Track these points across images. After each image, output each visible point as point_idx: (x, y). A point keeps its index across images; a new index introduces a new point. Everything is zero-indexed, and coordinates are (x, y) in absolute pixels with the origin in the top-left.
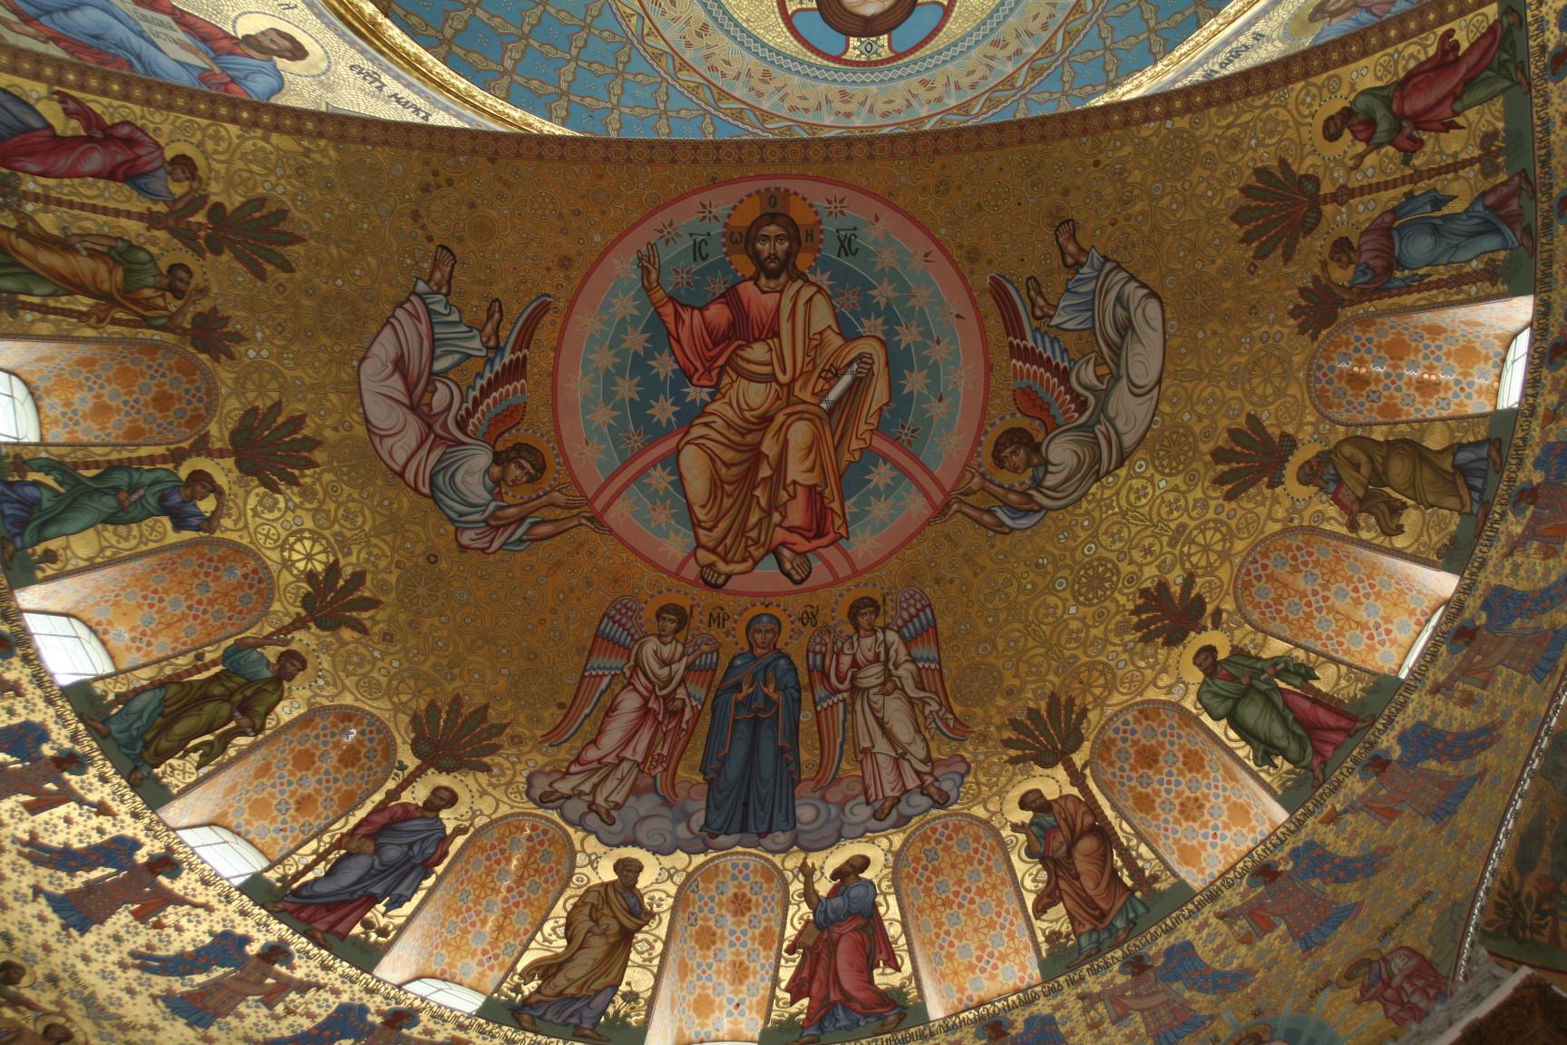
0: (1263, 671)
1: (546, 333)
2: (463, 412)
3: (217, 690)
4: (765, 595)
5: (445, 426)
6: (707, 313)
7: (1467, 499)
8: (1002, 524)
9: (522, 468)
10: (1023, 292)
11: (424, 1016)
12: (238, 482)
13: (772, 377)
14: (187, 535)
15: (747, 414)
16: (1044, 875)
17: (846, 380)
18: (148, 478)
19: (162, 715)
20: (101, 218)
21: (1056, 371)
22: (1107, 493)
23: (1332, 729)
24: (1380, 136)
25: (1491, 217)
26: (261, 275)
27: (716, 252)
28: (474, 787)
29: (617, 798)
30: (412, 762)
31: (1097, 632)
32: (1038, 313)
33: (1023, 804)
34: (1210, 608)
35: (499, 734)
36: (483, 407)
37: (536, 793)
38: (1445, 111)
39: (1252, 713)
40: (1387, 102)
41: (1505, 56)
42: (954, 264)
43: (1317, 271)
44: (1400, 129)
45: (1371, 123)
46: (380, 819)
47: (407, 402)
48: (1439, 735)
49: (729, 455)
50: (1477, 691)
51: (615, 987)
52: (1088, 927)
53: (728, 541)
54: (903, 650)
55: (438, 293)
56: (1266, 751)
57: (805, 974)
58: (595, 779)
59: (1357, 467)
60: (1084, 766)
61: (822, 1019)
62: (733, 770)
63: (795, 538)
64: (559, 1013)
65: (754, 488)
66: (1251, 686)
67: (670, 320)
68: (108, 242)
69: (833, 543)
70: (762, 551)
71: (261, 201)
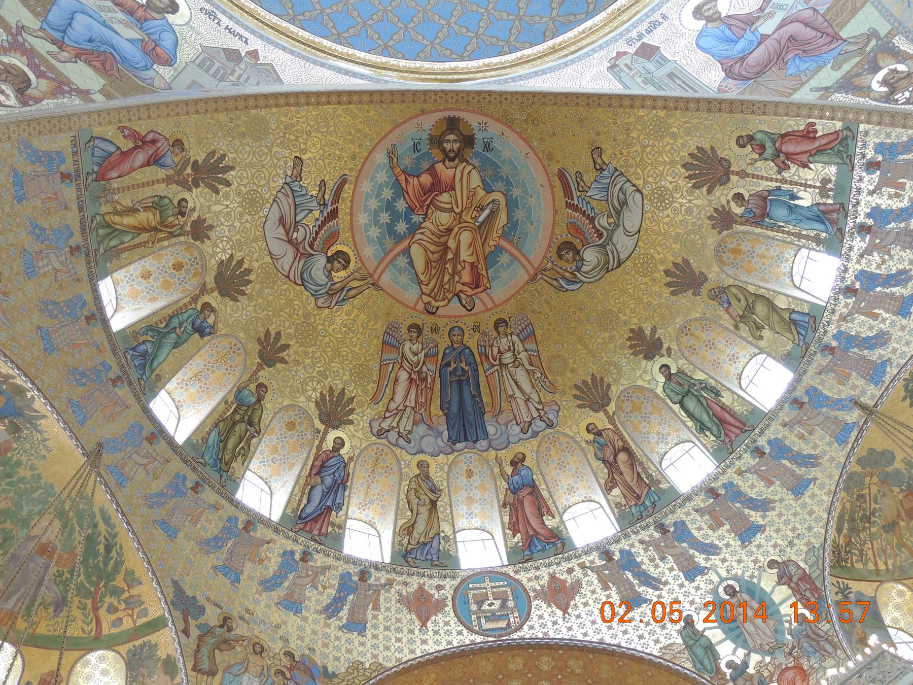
3: (238, 417)
4: (455, 317)
5: (304, 248)
7: (796, 337)
8: (563, 287)
9: (340, 262)
11: (372, 571)
13: (452, 210)
14: (206, 338)
15: (441, 228)
16: (606, 470)
17: (487, 212)
18: (186, 316)
19: (221, 441)
20: (146, 189)
23: (732, 425)
24: (766, 155)
25: (821, 215)
26: (217, 192)
27: (425, 147)
29: (409, 428)
30: (322, 427)
31: (611, 346)
32: (581, 189)
34: (665, 346)
35: (352, 403)
36: (320, 235)
37: (375, 431)
38: (804, 158)
39: (691, 404)
40: (774, 142)
41: (841, 148)
42: (541, 161)
44: (778, 156)
45: (763, 147)
46: (318, 463)
48: (789, 449)
50: (806, 434)
51: (439, 534)
52: (633, 503)
53: (436, 290)
54: (521, 346)
56: (702, 428)
57: (514, 520)
58: (397, 419)
59: (739, 301)
60: (614, 414)
61: (529, 545)
62: (455, 408)
63: (466, 288)
66: (689, 391)
67: (403, 183)
68: (150, 200)
69: (484, 291)
70: (451, 295)
71: (213, 153)
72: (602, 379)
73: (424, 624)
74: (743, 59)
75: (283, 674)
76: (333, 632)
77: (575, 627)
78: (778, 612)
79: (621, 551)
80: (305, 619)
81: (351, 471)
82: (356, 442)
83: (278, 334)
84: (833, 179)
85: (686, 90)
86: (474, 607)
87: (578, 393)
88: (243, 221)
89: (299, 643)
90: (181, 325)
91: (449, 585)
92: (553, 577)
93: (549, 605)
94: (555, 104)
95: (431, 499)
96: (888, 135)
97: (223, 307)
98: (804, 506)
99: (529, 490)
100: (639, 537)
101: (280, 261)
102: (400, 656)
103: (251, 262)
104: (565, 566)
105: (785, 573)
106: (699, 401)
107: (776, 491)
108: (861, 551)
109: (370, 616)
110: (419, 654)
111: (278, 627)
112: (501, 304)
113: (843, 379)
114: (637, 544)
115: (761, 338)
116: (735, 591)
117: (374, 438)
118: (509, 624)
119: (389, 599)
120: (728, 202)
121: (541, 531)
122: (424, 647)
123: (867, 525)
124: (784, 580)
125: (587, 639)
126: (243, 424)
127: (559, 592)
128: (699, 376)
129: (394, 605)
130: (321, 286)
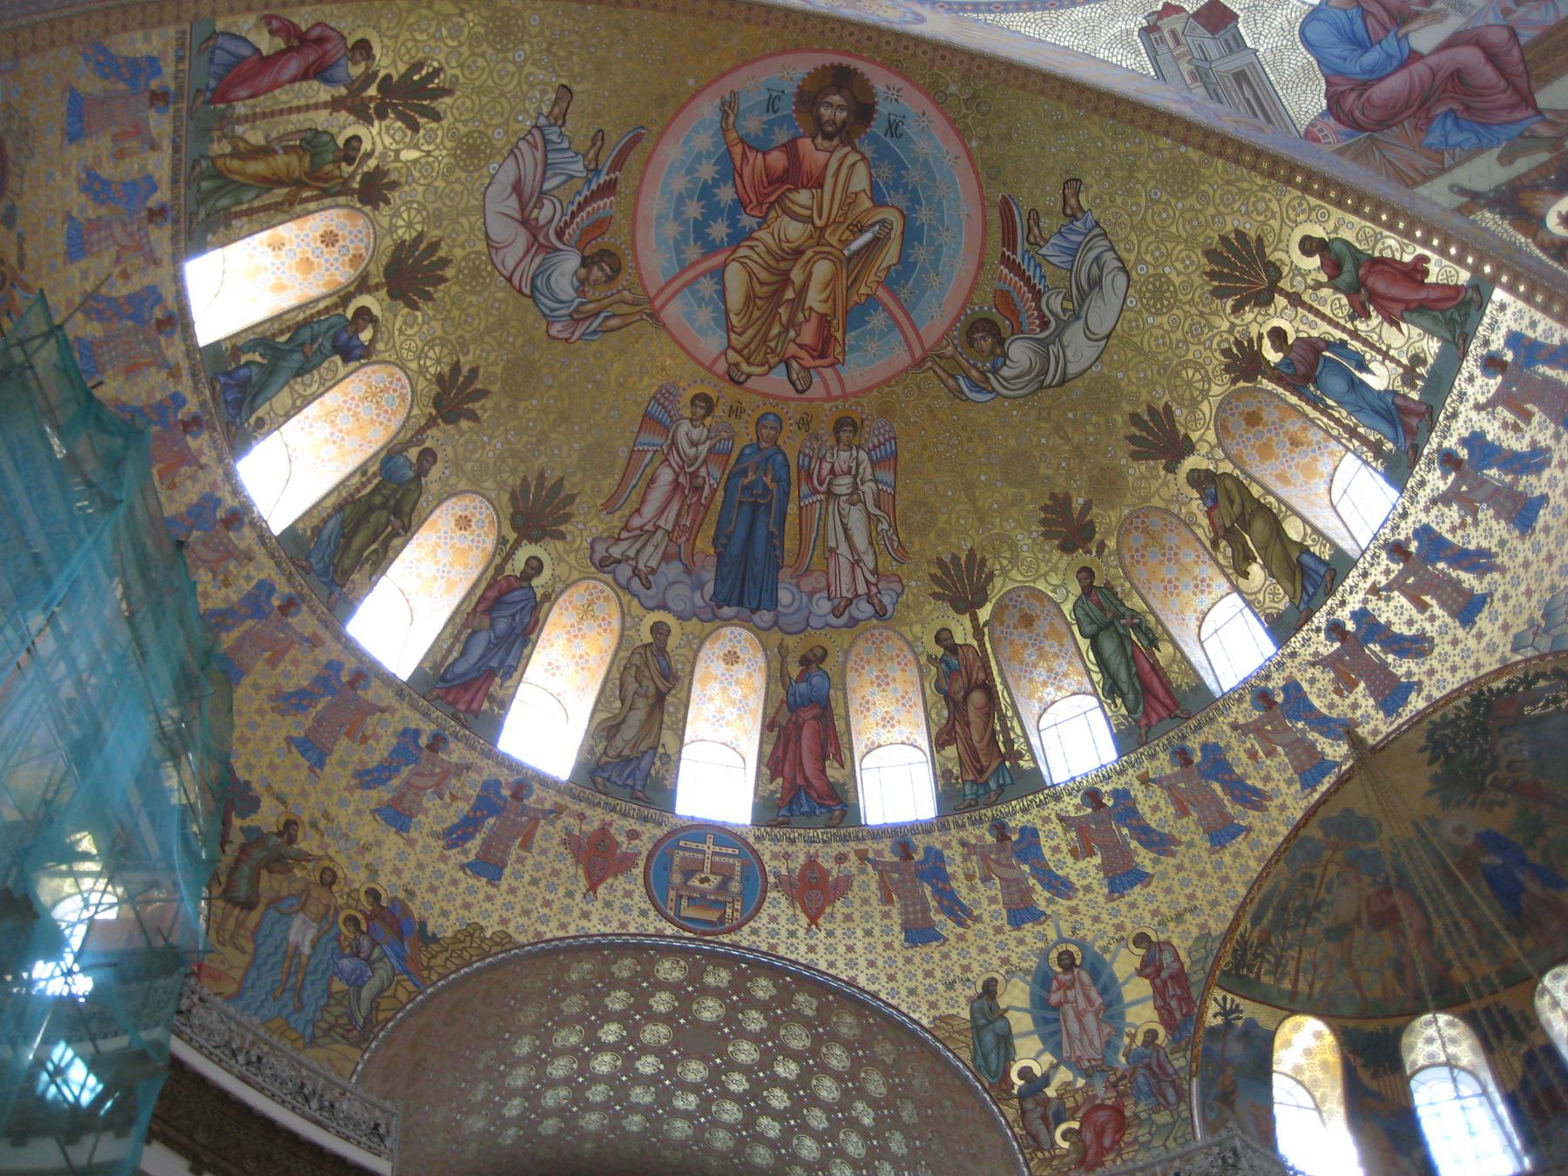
0: (1123, 616)
1: (634, 159)
4: (775, 397)
5: (547, 237)
7: (1298, 593)
8: (961, 391)
11: (536, 785)
12: (389, 309)
13: (810, 220)
15: (785, 245)
16: (946, 713)
17: (867, 237)
18: (324, 326)
19: (343, 536)
21: (1032, 288)
23: (1157, 699)
27: (787, 107)
28: (554, 554)
29: (653, 563)
30: (513, 537)
32: (1032, 239)
33: (938, 640)
34: (1097, 537)
36: (578, 219)
37: (597, 557)
38: (1397, 309)
39: (1109, 646)
42: (977, 174)
43: (1254, 335)
44: (1358, 291)
46: (493, 594)
49: (764, 276)
50: (1261, 754)
51: (655, 749)
52: (971, 777)
53: (752, 346)
54: (869, 470)
56: (1112, 689)
57: (780, 754)
58: (638, 545)
59: (1232, 503)
60: (985, 624)
61: (791, 802)
62: (736, 547)
63: (803, 354)
64: (620, 775)
66: (1112, 622)
67: (738, 158)
69: (832, 365)
72: (983, 560)
73: (593, 887)
74: (1365, 85)
75: (356, 922)
76: (450, 870)
77: (821, 950)
78: (1122, 1016)
79: (928, 850)
80: (411, 843)
81: (541, 616)
82: (562, 570)
83: (474, 372)
84: (1430, 361)
85: (1255, 115)
86: (677, 879)
87: (939, 573)
88: (452, 179)
89: (394, 878)
90: (313, 340)
91: (650, 834)
92: (812, 862)
93: (792, 905)
94: (1024, 87)
95: (657, 688)
96: (1533, 324)
97: (390, 317)
98: (1219, 865)
99: (817, 711)
100: (963, 834)
101: (502, 253)
102: (543, 928)
103: (451, 248)
104: (837, 848)
105: (1154, 959)
106: (1122, 645)
107: (1188, 830)
108: (1279, 958)
109: (513, 857)
110: (572, 931)
111: (365, 848)
112: (855, 395)
113: (1344, 684)
114: (954, 844)
115: (1246, 575)
116: (1073, 964)
117: (593, 569)
118: (722, 919)
119: (550, 836)
120: (1260, 337)
121: (817, 783)
122: (584, 923)
123: (1303, 921)
124: (1148, 971)
125: (832, 972)
126: (384, 513)
127: (812, 887)
128: (1136, 603)
129: (555, 847)
130: (561, 302)
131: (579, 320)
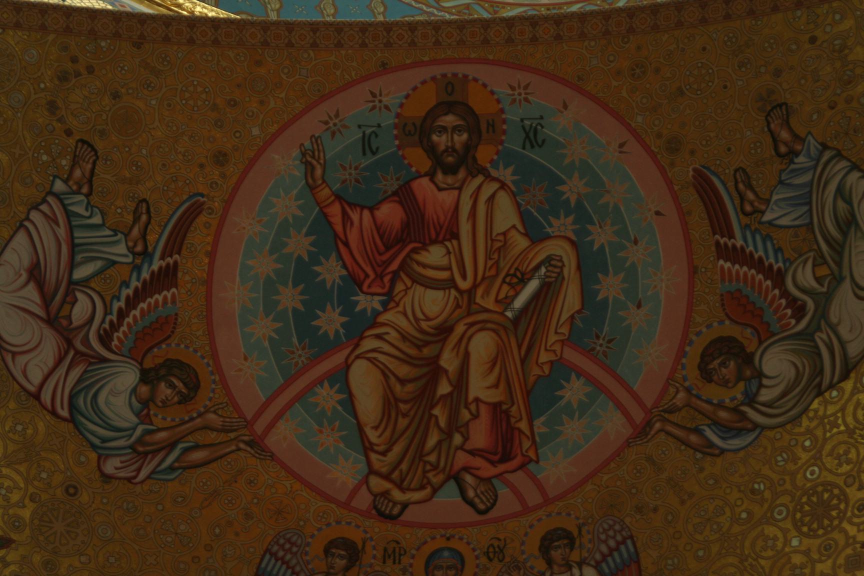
1: (199, 237)
2: (106, 326)
5: (86, 342)
6: (378, 213)
8: (711, 445)
10: (731, 184)
13: (451, 283)
15: (424, 325)
17: (533, 286)
21: (768, 272)
22: (831, 410)
32: (748, 208)
36: (130, 320)
47: (42, 314)
49: (403, 370)
53: (404, 466)
55: (78, 192)
63: (478, 462)
65: (432, 407)
67: (337, 220)
69: (522, 467)
70: (441, 477)
101: (22, 360)
112: (560, 497)
131: (146, 454)
